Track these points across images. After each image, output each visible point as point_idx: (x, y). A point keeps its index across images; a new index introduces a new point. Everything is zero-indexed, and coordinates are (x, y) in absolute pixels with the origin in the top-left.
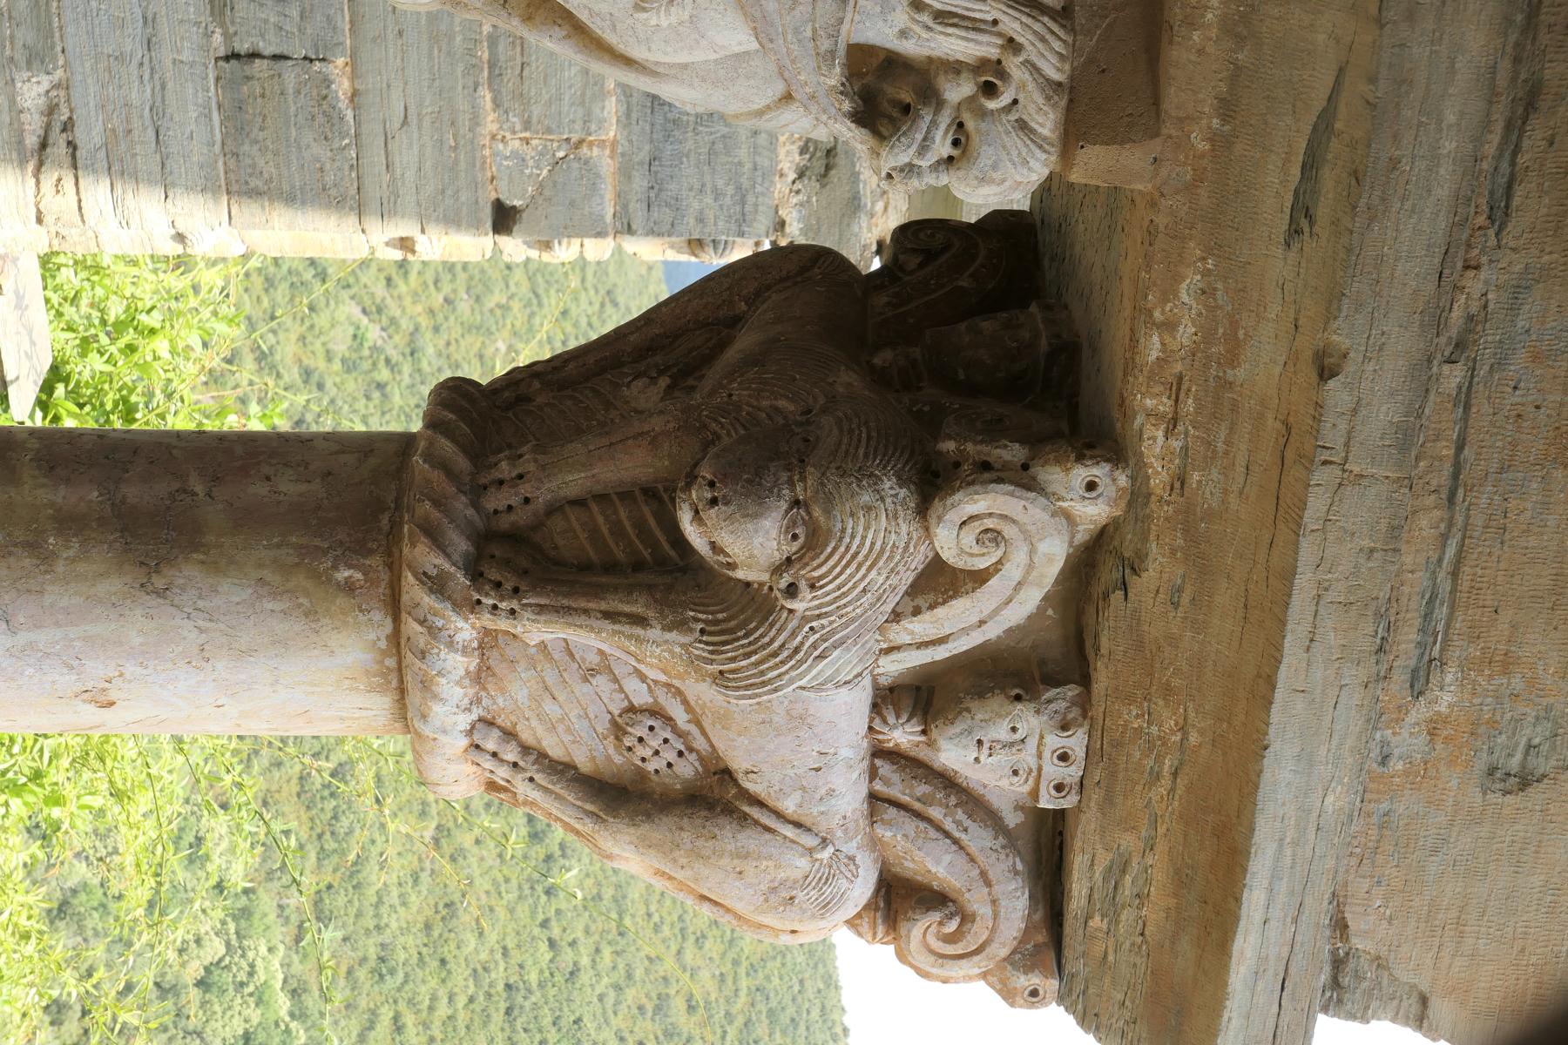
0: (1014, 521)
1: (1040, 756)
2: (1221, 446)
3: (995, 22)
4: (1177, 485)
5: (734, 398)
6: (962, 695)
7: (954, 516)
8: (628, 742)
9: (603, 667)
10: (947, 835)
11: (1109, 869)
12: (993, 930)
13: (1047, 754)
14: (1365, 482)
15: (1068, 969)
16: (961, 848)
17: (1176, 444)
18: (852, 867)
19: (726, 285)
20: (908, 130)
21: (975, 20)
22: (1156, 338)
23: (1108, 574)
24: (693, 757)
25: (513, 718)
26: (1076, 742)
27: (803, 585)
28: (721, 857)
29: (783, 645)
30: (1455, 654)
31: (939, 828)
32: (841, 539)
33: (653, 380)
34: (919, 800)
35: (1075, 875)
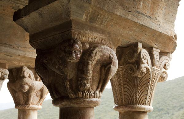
9: (34, 97)
23: (30, 67)
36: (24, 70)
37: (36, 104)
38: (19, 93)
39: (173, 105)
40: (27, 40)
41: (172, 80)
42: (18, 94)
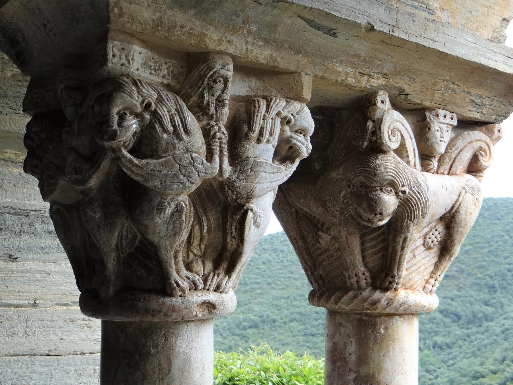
0: (390, 126)
1: (444, 124)
3: (272, 119)
4: (386, 76)
5: (338, 209)
6: (426, 146)
7: (389, 143)
8: (432, 246)
10: (459, 153)
11: (473, 107)
12: (483, 141)
13: (444, 121)
14: (398, 20)
15: (493, 120)
16: (462, 149)
17: (376, 75)
18: (469, 181)
19: (286, 215)
20: (298, 147)
21: (272, 125)
22: (349, 79)
24: (437, 227)
25: (423, 280)
26: (442, 112)
27: (403, 189)
28: (466, 219)
29: (417, 196)
31: (457, 155)
32: (393, 177)
33: (320, 236)
34: (450, 161)
35: (472, 116)
36: (378, 115)
37: (420, 284)
38: (343, 233)
42: (335, 238)
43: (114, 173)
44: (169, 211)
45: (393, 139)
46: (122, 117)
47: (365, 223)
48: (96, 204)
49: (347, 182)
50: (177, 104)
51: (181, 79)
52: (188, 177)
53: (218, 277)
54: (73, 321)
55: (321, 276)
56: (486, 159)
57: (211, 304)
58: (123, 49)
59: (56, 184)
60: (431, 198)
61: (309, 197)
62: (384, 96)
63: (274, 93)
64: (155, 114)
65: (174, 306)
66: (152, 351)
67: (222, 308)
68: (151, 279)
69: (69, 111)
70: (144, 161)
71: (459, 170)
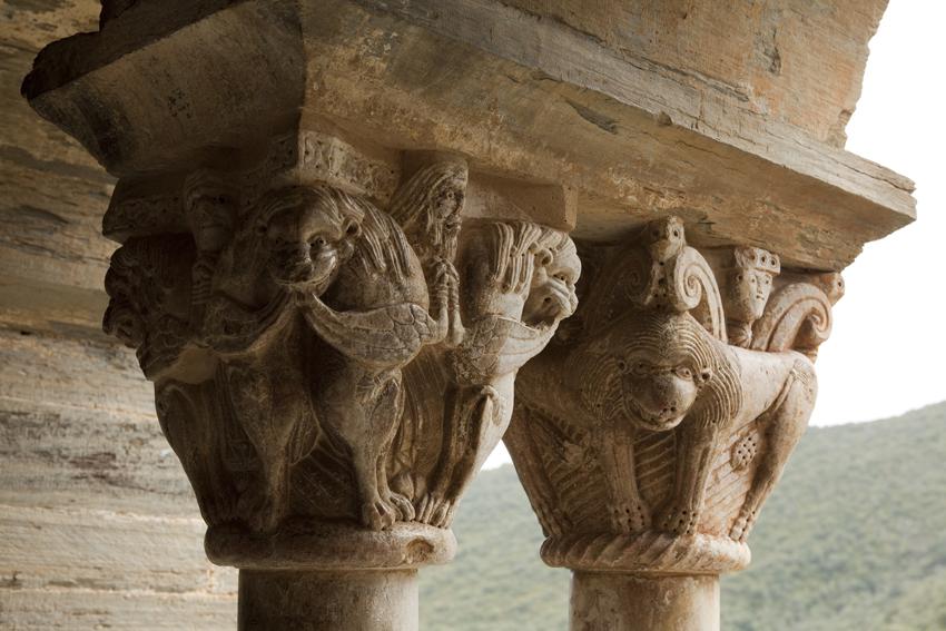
1: (762, 270)
2: (674, 173)
7: (685, 298)
10: (782, 317)
12: (818, 300)
13: (763, 267)
15: (831, 267)
17: (667, 193)
22: (630, 197)
23: (701, 231)
24: (751, 433)
26: (759, 253)
27: (705, 371)
30: (735, 81)
31: (780, 321)
33: (566, 449)
36: (669, 252)
37: (725, 525)
38: (609, 443)
39: (895, 544)
40: (685, 9)
41: (893, 420)
43: (289, 334)
44: (376, 391)
45: (691, 292)
46: (316, 247)
47: (646, 426)
48: (261, 381)
49: (617, 359)
50: (389, 224)
51: (392, 191)
52: (407, 341)
53: (435, 502)
54: (78, 613)
55: (566, 517)
56: (822, 328)
57: (427, 544)
58: (320, 143)
59: (178, 350)
60: (746, 387)
61: (552, 384)
62: (677, 225)
63: (523, 215)
64: (361, 242)
65: (375, 543)
66: (335, 617)
67: (440, 551)
68: (337, 502)
69: (206, 238)
70: (345, 314)
71: (783, 344)
